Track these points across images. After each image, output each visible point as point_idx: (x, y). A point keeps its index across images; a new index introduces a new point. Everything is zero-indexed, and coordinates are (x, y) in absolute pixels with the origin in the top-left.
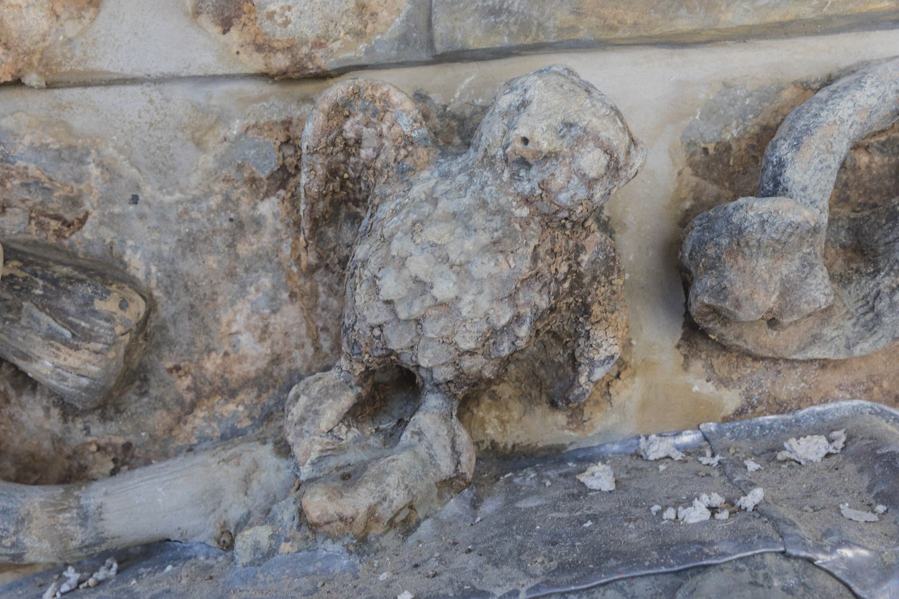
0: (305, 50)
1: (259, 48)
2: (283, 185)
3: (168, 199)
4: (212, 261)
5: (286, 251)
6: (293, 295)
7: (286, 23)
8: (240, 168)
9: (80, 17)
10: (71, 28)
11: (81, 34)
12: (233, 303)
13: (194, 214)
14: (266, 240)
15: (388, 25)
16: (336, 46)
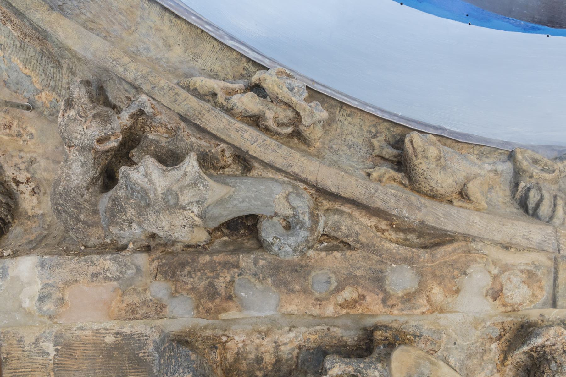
0: (516, 306)
1: (504, 306)
2: (499, 340)
3: (465, 344)
4: (475, 361)
5: (497, 357)
6: (498, 371)
7: (512, 299)
8: (487, 335)
9: (453, 297)
10: (450, 300)
11: (452, 301)
12: (480, 373)
13: (472, 348)
14: (492, 355)
15: (540, 299)
16: (525, 305)
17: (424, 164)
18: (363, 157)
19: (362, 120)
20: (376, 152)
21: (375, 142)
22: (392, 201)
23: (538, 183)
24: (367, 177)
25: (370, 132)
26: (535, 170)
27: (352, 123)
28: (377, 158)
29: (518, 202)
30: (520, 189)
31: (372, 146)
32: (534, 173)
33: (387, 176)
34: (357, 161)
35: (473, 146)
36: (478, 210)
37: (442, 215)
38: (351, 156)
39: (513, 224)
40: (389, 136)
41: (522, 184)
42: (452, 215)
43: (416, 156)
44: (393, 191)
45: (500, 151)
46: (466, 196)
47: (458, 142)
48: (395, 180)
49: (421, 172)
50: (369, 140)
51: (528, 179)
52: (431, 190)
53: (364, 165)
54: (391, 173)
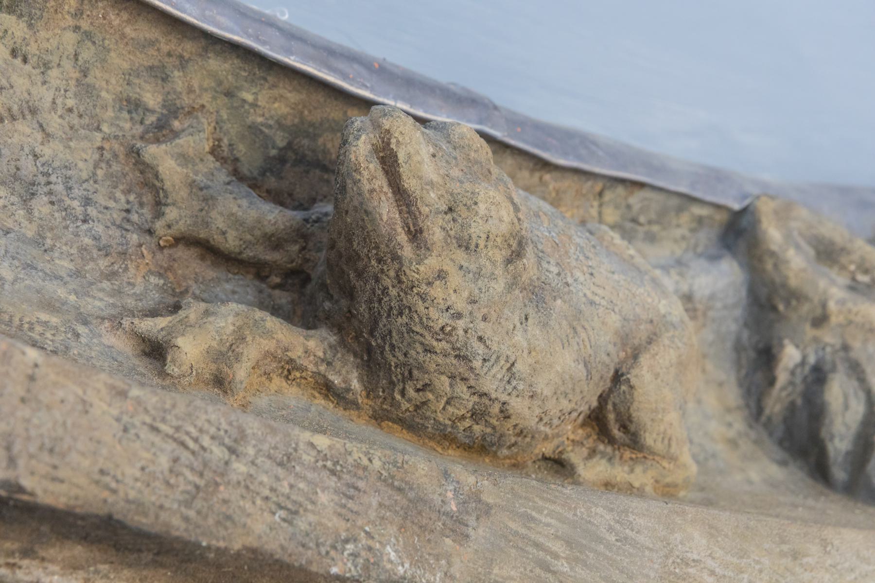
17: (455, 279)
18: (105, 251)
19: (88, 35)
20: (178, 216)
21: (164, 158)
22: (324, 498)
23: (846, 348)
24: (142, 365)
25: (134, 106)
26: (831, 288)
27: (33, 49)
28: (182, 253)
29: (779, 432)
30: (782, 377)
31: (149, 185)
32: (832, 306)
33: (251, 352)
34: (78, 274)
35: (599, 186)
36: (667, 492)
37: (557, 547)
38: (38, 241)
39: (825, 543)
40: (233, 129)
41: (790, 355)
42: (600, 540)
43: (415, 235)
44: (322, 441)
45: (698, 211)
46: (624, 427)
47: (545, 165)
48: (289, 369)
49: (440, 319)
50: (134, 153)
51: (810, 332)
52: (477, 415)
53: (119, 292)
54: (268, 334)
